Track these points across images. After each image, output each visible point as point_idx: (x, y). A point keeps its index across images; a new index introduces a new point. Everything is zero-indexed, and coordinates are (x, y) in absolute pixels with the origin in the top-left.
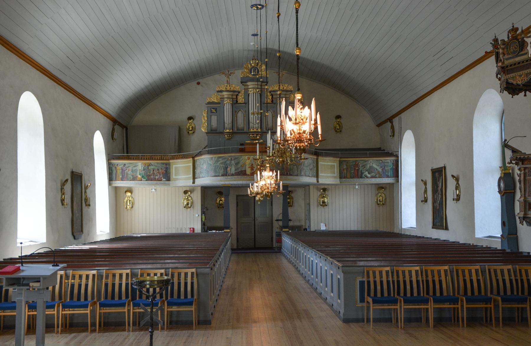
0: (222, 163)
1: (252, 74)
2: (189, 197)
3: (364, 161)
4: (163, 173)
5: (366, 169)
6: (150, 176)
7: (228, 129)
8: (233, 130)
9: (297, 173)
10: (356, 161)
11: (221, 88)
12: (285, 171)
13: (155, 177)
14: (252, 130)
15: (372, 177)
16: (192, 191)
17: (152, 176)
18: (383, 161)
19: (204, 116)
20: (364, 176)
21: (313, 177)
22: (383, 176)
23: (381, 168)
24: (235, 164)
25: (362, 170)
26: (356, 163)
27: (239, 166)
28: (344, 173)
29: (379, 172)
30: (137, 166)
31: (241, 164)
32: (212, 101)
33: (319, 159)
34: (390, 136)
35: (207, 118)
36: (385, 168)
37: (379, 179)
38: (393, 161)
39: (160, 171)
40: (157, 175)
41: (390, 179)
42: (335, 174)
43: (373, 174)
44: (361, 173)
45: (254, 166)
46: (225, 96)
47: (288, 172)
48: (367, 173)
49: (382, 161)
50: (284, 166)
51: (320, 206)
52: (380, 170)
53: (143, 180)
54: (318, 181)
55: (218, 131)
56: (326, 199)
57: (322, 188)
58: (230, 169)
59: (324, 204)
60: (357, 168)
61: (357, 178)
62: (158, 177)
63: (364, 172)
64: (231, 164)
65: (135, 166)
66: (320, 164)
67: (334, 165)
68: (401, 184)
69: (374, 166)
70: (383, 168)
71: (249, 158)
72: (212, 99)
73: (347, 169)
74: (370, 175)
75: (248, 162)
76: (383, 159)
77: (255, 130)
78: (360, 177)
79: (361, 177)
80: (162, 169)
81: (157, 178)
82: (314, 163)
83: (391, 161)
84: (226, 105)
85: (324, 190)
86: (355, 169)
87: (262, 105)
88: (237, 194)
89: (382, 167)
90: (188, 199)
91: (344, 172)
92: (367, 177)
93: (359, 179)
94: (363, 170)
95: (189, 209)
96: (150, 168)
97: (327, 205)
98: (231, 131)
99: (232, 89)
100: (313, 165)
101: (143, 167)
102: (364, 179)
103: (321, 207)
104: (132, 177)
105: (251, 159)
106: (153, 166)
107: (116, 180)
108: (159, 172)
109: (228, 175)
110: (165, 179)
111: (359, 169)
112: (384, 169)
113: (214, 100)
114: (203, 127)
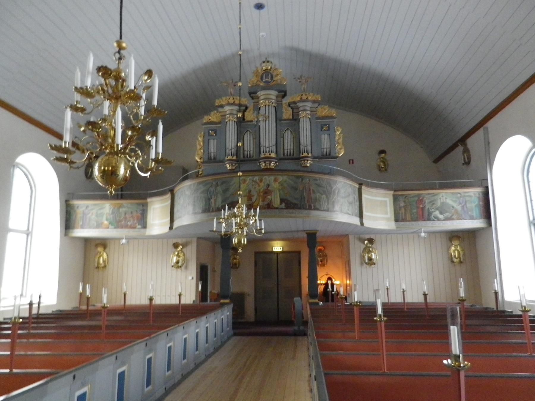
0: (202, 192)
1: (264, 80)
3: (432, 195)
5: (435, 207)
6: (120, 221)
7: (230, 154)
8: (237, 158)
9: (327, 207)
10: (419, 195)
12: (306, 202)
14: (262, 156)
15: (446, 219)
16: (184, 245)
18: (463, 194)
19: (199, 141)
20: (434, 217)
21: (353, 216)
22: (463, 216)
23: (461, 205)
24: (223, 192)
25: (430, 208)
26: (419, 198)
28: (402, 213)
29: (456, 211)
31: (232, 190)
32: (210, 121)
33: (362, 189)
35: (204, 143)
36: (466, 205)
37: (458, 221)
38: (479, 194)
39: (135, 214)
41: (475, 221)
43: (448, 214)
44: (429, 213)
45: (254, 193)
46: (228, 112)
48: (437, 213)
51: (365, 264)
53: (110, 227)
54: (362, 224)
55: (217, 160)
56: (373, 254)
58: (215, 201)
59: (371, 262)
60: (421, 206)
63: (433, 212)
66: (365, 197)
67: (386, 202)
68: (496, 229)
69: (449, 201)
70: (463, 205)
73: (405, 207)
77: (267, 155)
78: (426, 219)
79: (429, 219)
82: (355, 195)
83: (475, 194)
84: (228, 123)
85: (371, 241)
86: (418, 207)
87: (278, 122)
89: (460, 204)
90: (178, 256)
91: (401, 212)
92: (438, 219)
93: (425, 222)
95: (179, 270)
97: (374, 264)
98: (235, 158)
100: (354, 198)
103: (367, 265)
104: (95, 224)
107: (78, 228)
109: (211, 210)
111: (425, 206)
112: (465, 206)
113: (214, 119)
114: (198, 154)
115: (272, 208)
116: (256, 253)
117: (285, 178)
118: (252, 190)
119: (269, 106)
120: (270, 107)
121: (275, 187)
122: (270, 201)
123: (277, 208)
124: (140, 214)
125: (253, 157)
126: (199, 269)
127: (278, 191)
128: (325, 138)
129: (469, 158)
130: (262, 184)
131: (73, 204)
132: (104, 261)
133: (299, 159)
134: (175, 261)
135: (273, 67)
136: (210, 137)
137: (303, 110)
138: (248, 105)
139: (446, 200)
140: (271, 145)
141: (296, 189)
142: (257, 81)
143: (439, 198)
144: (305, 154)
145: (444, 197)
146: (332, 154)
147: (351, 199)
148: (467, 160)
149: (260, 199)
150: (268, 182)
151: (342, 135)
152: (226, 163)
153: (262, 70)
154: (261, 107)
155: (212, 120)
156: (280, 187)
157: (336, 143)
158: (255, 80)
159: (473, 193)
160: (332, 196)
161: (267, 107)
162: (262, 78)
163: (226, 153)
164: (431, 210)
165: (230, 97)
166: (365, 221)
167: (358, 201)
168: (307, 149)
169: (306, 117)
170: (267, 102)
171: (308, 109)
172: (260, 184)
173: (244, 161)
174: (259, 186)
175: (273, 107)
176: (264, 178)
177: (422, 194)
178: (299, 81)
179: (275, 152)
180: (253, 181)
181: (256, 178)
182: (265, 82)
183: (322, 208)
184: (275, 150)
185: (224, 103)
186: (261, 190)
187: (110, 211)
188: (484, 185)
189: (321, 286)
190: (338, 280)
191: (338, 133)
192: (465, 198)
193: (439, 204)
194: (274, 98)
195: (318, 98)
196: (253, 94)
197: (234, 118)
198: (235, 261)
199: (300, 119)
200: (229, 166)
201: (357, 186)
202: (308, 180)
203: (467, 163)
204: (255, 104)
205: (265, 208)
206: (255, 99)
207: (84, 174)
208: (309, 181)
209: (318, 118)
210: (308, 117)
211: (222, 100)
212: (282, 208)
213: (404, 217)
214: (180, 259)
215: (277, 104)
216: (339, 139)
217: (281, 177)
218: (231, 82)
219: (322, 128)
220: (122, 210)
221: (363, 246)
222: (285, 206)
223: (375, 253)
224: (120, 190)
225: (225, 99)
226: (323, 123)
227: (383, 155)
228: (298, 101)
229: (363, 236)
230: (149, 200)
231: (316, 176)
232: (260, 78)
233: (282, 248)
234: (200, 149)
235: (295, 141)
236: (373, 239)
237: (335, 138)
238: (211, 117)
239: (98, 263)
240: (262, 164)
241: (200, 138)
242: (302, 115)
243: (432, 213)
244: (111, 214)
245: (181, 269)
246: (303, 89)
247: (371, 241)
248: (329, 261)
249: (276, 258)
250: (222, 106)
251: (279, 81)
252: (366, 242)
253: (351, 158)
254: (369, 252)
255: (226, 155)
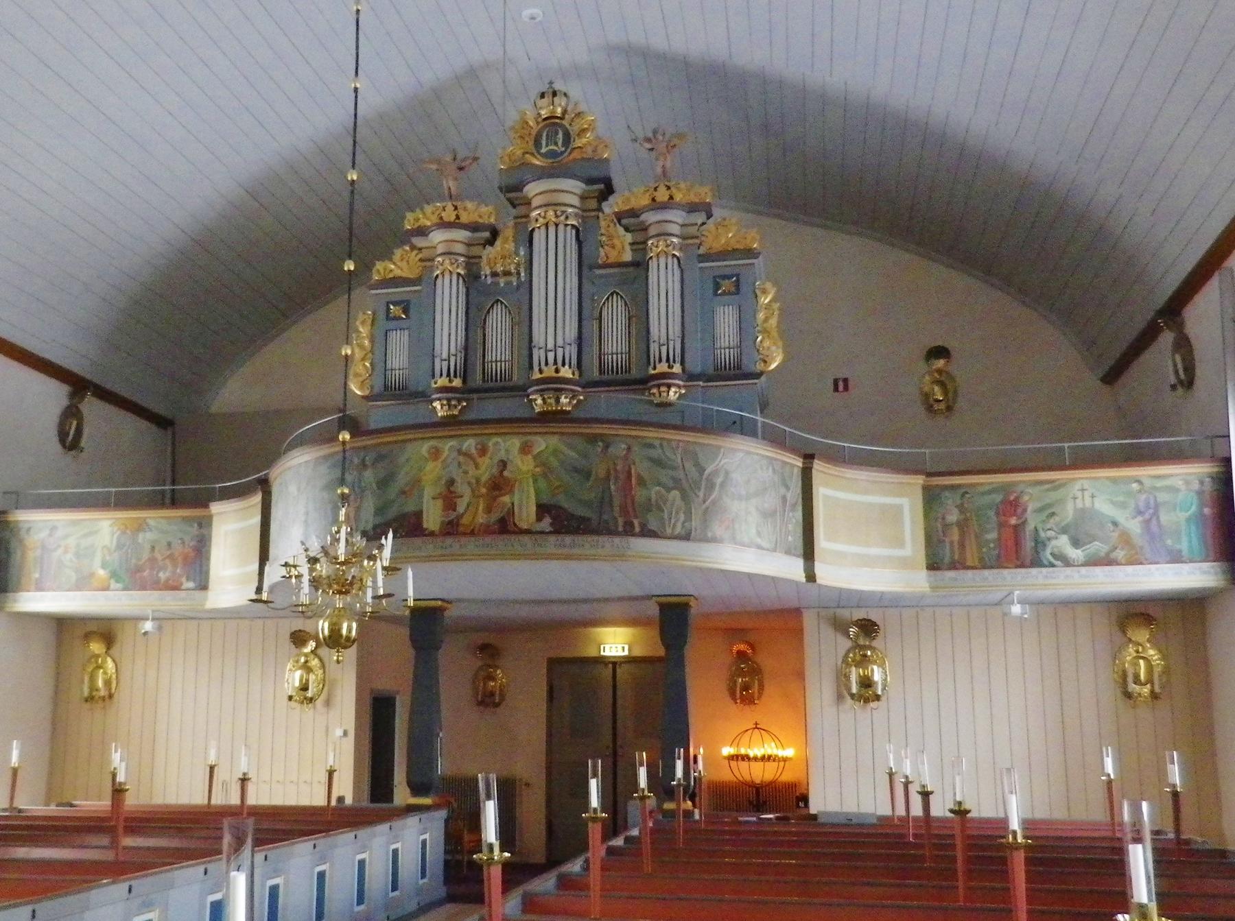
1: (543, 150)
2: (312, 656)
3: (1047, 486)
4: (185, 558)
5: (1057, 525)
9: (683, 526)
10: (1005, 488)
11: (422, 220)
13: (158, 573)
14: (536, 375)
17: (147, 571)
18: (1148, 483)
23: (1140, 518)
24: (377, 483)
27: (393, 491)
28: (952, 543)
29: (1126, 539)
30: (96, 532)
31: (402, 479)
33: (813, 471)
34: (1173, 387)
36: (1158, 518)
37: (1130, 569)
38: (1202, 483)
40: (164, 568)
42: (900, 543)
45: (463, 489)
47: (636, 517)
48: (1063, 543)
49: (1139, 482)
50: (612, 487)
51: (849, 700)
52: (1134, 526)
54: (811, 577)
57: (855, 619)
59: (867, 692)
60: (1013, 521)
61: (1017, 567)
62: (168, 574)
63: (1049, 539)
64: (359, 487)
65: (86, 536)
66: (826, 497)
67: (899, 508)
69: (1104, 507)
70: (1147, 516)
71: (436, 454)
72: (393, 267)
73: (962, 525)
74: (1079, 552)
75: (432, 471)
76: (1145, 473)
77: (549, 372)
79: (1036, 563)
80: (184, 543)
81: (162, 581)
82: (788, 488)
83: (1187, 483)
85: (868, 628)
86: (1002, 525)
87: (585, 271)
88: (553, 654)
89: (1140, 513)
90: (307, 668)
92: (1067, 562)
93: (1023, 570)
94: (1045, 530)
96: (140, 541)
97: (878, 698)
98: (457, 383)
99: (465, 218)
100: (784, 499)
101: (115, 536)
102: (1051, 569)
105: (446, 453)
106: (151, 530)
108: (171, 557)
110: (194, 581)
111: (1024, 523)
112: (1154, 521)
114: (357, 375)
115: (514, 533)
116: (555, 664)
117: (554, 441)
118: (458, 480)
119: (557, 225)
120: (561, 227)
121: (524, 468)
122: (509, 509)
123: (528, 532)
124: (191, 550)
125: (629, 370)
126: (368, 709)
127: (531, 480)
128: (726, 320)
129: (1190, 369)
130: (485, 462)
131: (17, 522)
132: (107, 683)
133: (644, 382)
134: (297, 684)
135: (569, 109)
136: (392, 324)
137: (658, 235)
138: (500, 226)
139: (1093, 503)
140: (560, 342)
141: (587, 475)
142: (524, 153)
143: (1071, 495)
144: (662, 367)
145: (1086, 493)
146: (749, 365)
147: (770, 501)
148: (1182, 376)
149: (478, 505)
150: (502, 455)
151: (776, 306)
152: (434, 396)
153: (540, 120)
154: (533, 230)
155: (398, 273)
156: (538, 469)
157: (759, 332)
158: (516, 149)
159: (1184, 479)
160: (701, 494)
161: (552, 229)
162: (537, 143)
163: (433, 369)
164: (1042, 534)
165: (444, 204)
166: (820, 569)
167: (800, 508)
168: (564, 356)
169: (667, 257)
170: (551, 213)
171: (675, 229)
172: (480, 460)
173: (486, 390)
174: (477, 466)
175: (569, 227)
176: (490, 444)
177: (1015, 484)
178: (648, 146)
179: (574, 362)
180: (460, 452)
181: (470, 444)
182: (545, 155)
183: (669, 531)
184: (574, 357)
185: (429, 223)
186: (484, 479)
187: (112, 541)
188: (1221, 454)
189: (739, 763)
190: (789, 746)
191: (765, 300)
192: (1155, 497)
193: (1068, 512)
194: (575, 201)
195: (703, 194)
196: (512, 191)
197: (456, 265)
198: (492, 684)
199: (650, 262)
200: (442, 408)
201: (799, 463)
202: (623, 446)
203: (1188, 381)
204: (519, 220)
205: (493, 533)
206: (518, 208)
207: (56, 432)
208: (629, 449)
209: (704, 258)
210: (674, 255)
211: (424, 214)
212: (542, 533)
213: (956, 557)
214: (312, 677)
215: (583, 217)
216: (766, 320)
217: (542, 441)
218: (448, 158)
219: (717, 286)
220: (145, 538)
221: (845, 644)
222: (551, 524)
223: (882, 665)
224: (169, 480)
225: (430, 211)
226: (717, 273)
227: (940, 363)
228: (645, 207)
229: (845, 614)
230: (216, 508)
231: (651, 434)
232: (531, 143)
233: (626, 647)
234: (363, 359)
235: (634, 332)
236: (875, 624)
237: (755, 313)
238: (394, 264)
239: (93, 687)
240: (535, 400)
241: (363, 327)
242: (654, 249)
243: (1048, 543)
244: (115, 551)
245: (315, 708)
246: (659, 170)
247: (868, 628)
248: (769, 689)
249: (610, 679)
250: (422, 232)
251: (589, 152)
252: (853, 630)
253: (841, 376)
254: (864, 661)
255: (433, 376)
